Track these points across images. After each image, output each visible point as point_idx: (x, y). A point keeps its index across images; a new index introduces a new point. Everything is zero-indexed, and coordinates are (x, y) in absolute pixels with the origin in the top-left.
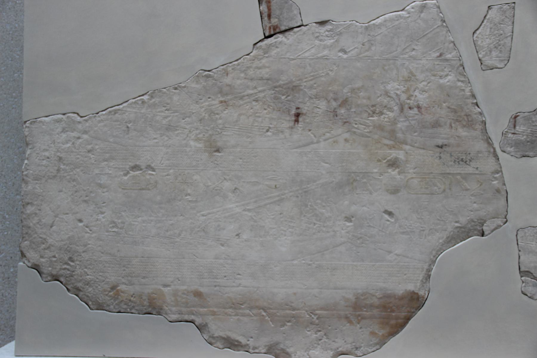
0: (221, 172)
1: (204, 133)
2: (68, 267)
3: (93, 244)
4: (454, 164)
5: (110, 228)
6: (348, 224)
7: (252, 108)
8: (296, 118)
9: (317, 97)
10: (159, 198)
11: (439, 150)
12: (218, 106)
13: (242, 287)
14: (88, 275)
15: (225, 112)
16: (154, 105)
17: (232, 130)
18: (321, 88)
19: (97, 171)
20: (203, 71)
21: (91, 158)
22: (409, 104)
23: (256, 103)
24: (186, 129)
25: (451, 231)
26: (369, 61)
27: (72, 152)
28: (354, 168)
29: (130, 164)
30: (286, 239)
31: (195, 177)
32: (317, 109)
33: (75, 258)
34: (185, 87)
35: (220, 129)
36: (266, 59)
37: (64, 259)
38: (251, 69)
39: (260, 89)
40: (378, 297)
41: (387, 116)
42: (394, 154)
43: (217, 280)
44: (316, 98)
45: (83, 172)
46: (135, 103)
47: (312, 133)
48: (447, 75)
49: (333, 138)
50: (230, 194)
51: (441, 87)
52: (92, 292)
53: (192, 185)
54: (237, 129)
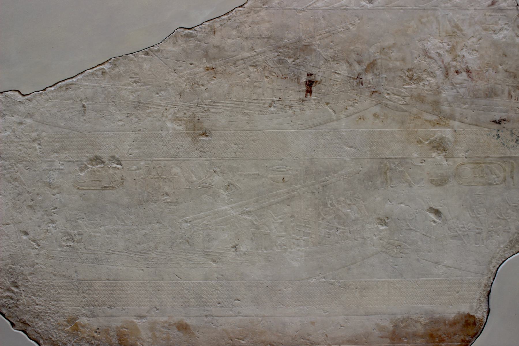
0: (209, 162)
1: (185, 111)
2: (11, 294)
3: (42, 263)
4: (516, 144)
5: (64, 241)
6: (382, 228)
8: (308, 87)
9: (335, 59)
10: (126, 200)
11: (496, 126)
12: (203, 74)
13: (242, 316)
14: (37, 305)
15: (213, 82)
16: (119, 76)
17: (223, 106)
18: (340, 48)
19: (44, 166)
20: (182, 29)
21: (36, 150)
22: (455, 67)
24: (161, 106)
25: (516, 233)
26: (402, 11)
27: (12, 142)
28: (387, 153)
29: (88, 155)
30: (299, 250)
31: (175, 170)
32: (336, 75)
33: (20, 283)
34: (158, 51)
35: (206, 105)
36: (266, 11)
37: (5, 284)
38: (246, 25)
39: (258, 50)
40: (423, 323)
41: (427, 83)
42: (439, 132)
43: (208, 308)
44: (333, 61)
45: (27, 168)
46: (93, 74)
47: (331, 108)
48: (501, 29)
49: (359, 112)
50: (222, 191)
51: (495, 44)
52: (43, 327)
53: (171, 181)
54: (228, 104)
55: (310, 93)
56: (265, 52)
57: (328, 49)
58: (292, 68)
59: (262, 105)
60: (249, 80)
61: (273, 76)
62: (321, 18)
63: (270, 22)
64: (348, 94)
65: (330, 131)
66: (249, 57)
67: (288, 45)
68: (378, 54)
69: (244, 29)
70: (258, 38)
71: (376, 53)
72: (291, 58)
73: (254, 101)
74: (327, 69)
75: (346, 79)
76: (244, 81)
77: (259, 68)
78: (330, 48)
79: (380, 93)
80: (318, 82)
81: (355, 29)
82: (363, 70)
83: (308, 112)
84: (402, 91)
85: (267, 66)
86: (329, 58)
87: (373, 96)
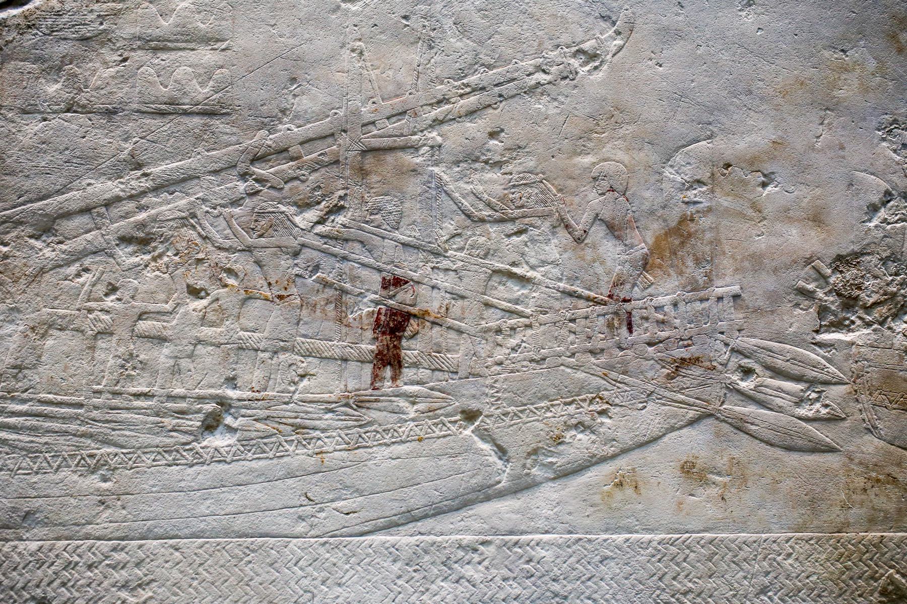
7: (113, 289)
18: (531, 163)
23: (133, 254)
44: (501, 221)
47: (485, 435)
49: (614, 457)
56: (191, 178)
57: (477, 165)
58: (315, 254)
60: (118, 306)
61: (226, 286)
62: (448, 23)
63: (218, 40)
64: (569, 370)
65: (483, 543)
66: (118, 199)
67: (294, 150)
68: (704, 188)
76: (90, 311)
78: (486, 162)
80: (432, 319)
81: (599, 75)
82: (633, 263)
84: (813, 356)
85: (199, 241)
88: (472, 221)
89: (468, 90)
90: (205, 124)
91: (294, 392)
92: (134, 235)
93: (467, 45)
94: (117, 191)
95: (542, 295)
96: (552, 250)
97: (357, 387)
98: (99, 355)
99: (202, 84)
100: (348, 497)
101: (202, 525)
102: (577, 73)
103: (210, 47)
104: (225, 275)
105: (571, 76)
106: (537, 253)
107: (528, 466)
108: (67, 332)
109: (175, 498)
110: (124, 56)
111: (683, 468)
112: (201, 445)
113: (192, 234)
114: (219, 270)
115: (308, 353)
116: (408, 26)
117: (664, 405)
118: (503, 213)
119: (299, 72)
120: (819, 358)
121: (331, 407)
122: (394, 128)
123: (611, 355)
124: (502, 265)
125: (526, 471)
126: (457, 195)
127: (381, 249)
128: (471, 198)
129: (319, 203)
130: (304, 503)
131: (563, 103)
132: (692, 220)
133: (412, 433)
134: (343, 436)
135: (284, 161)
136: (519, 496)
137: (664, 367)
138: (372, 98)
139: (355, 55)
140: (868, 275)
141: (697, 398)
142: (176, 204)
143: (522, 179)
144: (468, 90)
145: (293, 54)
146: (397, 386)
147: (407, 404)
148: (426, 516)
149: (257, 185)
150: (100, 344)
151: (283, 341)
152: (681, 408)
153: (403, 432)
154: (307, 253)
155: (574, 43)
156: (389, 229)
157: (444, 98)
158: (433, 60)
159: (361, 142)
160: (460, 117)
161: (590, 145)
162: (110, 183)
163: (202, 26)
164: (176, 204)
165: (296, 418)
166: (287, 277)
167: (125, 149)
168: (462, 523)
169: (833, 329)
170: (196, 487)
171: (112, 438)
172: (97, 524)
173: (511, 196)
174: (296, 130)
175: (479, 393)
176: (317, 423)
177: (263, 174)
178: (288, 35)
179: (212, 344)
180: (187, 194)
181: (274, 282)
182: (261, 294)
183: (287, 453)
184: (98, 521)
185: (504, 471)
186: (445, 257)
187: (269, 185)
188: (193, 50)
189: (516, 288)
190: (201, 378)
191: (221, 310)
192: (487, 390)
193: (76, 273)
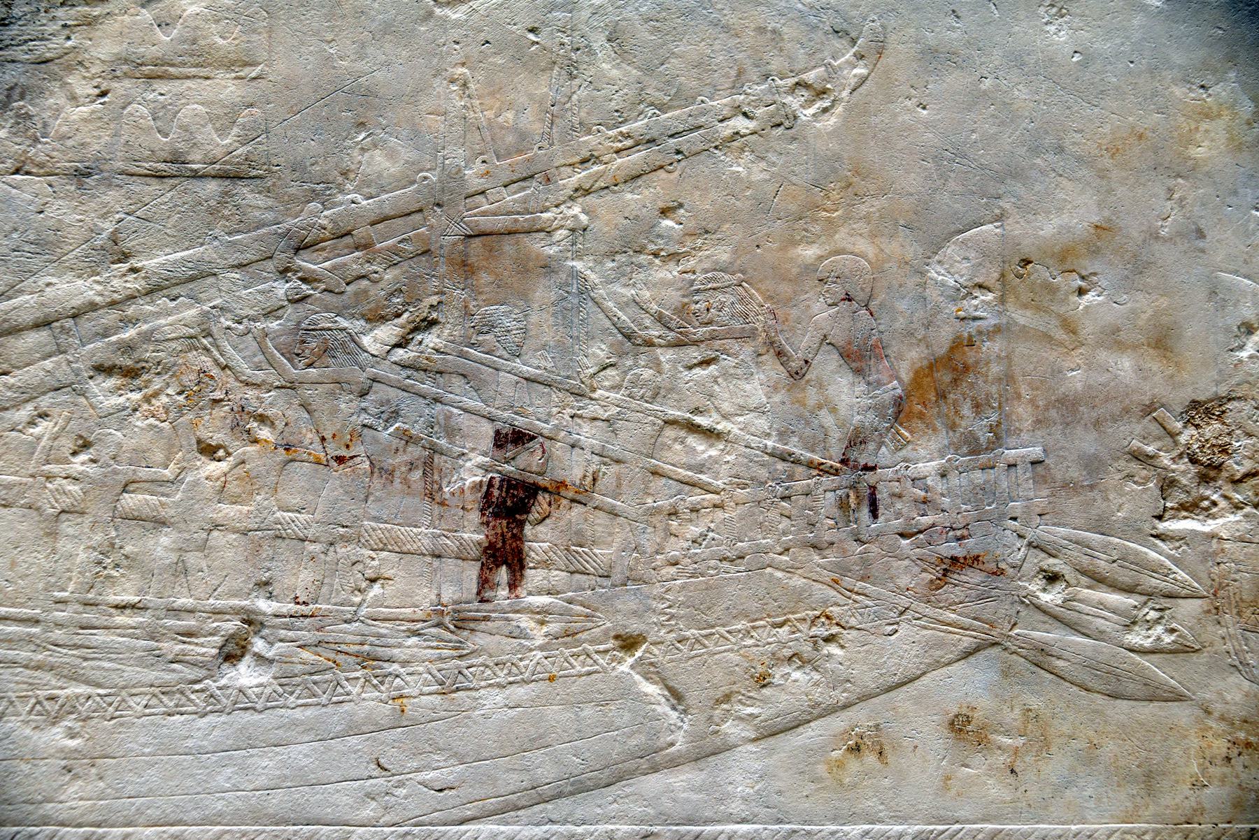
18: (723, 255)
23: (116, 390)
32: (692, 440)
39: (153, 262)
44: (678, 344)
47: (650, 671)
55: (509, 566)
56: (203, 276)
58: (393, 393)
59: (171, 647)
60: (92, 470)
61: (256, 441)
62: (599, 41)
63: (246, 64)
64: (779, 574)
66: (93, 307)
68: (990, 297)
69: (58, 111)
70: (161, 177)
71: (977, 293)
72: (383, 319)
73: (121, 619)
74: (634, 404)
75: (763, 473)
76: (49, 477)
77: (157, 384)
78: (656, 255)
79: (999, 573)
80: (571, 494)
81: (831, 121)
82: (879, 409)
83: (493, 699)
84: (1153, 555)
85: (215, 372)
86: (647, 322)
87: (950, 593)
88: (634, 344)
89: (629, 143)
90: (226, 193)
91: (360, 605)
92: (117, 362)
93: (627, 74)
94: (91, 295)
95: (740, 459)
96: (755, 390)
97: (455, 597)
98: (64, 545)
99: (222, 132)
100: (441, 764)
101: (219, 805)
102: (795, 118)
103: (233, 75)
104: (255, 424)
105: (787, 124)
106: (733, 394)
107: (716, 719)
108: (13, 510)
109: (178, 763)
110: (103, 89)
111: (952, 723)
112: (217, 684)
113: (206, 361)
114: (246, 417)
115: (381, 545)
116: (537, 43)
117: (925, 628)
118: (681, 333)
119: (370, 114)
120: (1162, 558)
121: (415, 628)
122: (515, 201)
123: (844, 551)
124: (679, 413)
125: (714, 727)
126: (611, 304)
127: (494, 386)
128: (633, 309)
129: (398, 316)
130: (375, 774)
131: (774, 164)
132: (971, 344)
133: (539, 668)
134: (435, 672)
135: (346, 251)
136: (702, 764)
137: (924, 570)
138: (481, 154)
139: (455, 88)
140: (1238, 432)
141: (975, 619)
142: (180, 316)
143: (710, 280)
144: (629, 143)
145: (360, 86)
146: (517, 597)
147: (533, 624)
148: (560, 795)
149: (304, 287)
150: (67, 527)
151: (343, 527)
152: (950, 632)
153: (526, 667)
154: (380, 392)
155: (791, 71)
156: (506, 356)
157: (592, 155)
158: (575, 97)
159: (464, 223)
160: (616, 185)
161: (816, 228)
162: (80, 282)
163: (221, 42)
164: (180, 316)
165: (362, 644)
166: (350, 429)
167: (103, 230)
168: (615, 805)
169: (1185, 514)
170: (211, 748)
171: (83, 672)
172: (61, 802)
173: (693, 307)
174: (365, 202)
175: (642, 608)
176: (396, 651)
177: (314, 271)
178: (352, 57)
179: (236, 531)
180: (198, 301)
181: (330, 436)
182: (310, 454)
183: (348, 698)
184: (62, 798)
185: (680, 728)
186: (591, 399)
187: (323, 286)
188: (207, 78)
189: (701, 448)
190: (217, 583)
191: (249, 478)
192: (654, 604)
193: (28, 419)
